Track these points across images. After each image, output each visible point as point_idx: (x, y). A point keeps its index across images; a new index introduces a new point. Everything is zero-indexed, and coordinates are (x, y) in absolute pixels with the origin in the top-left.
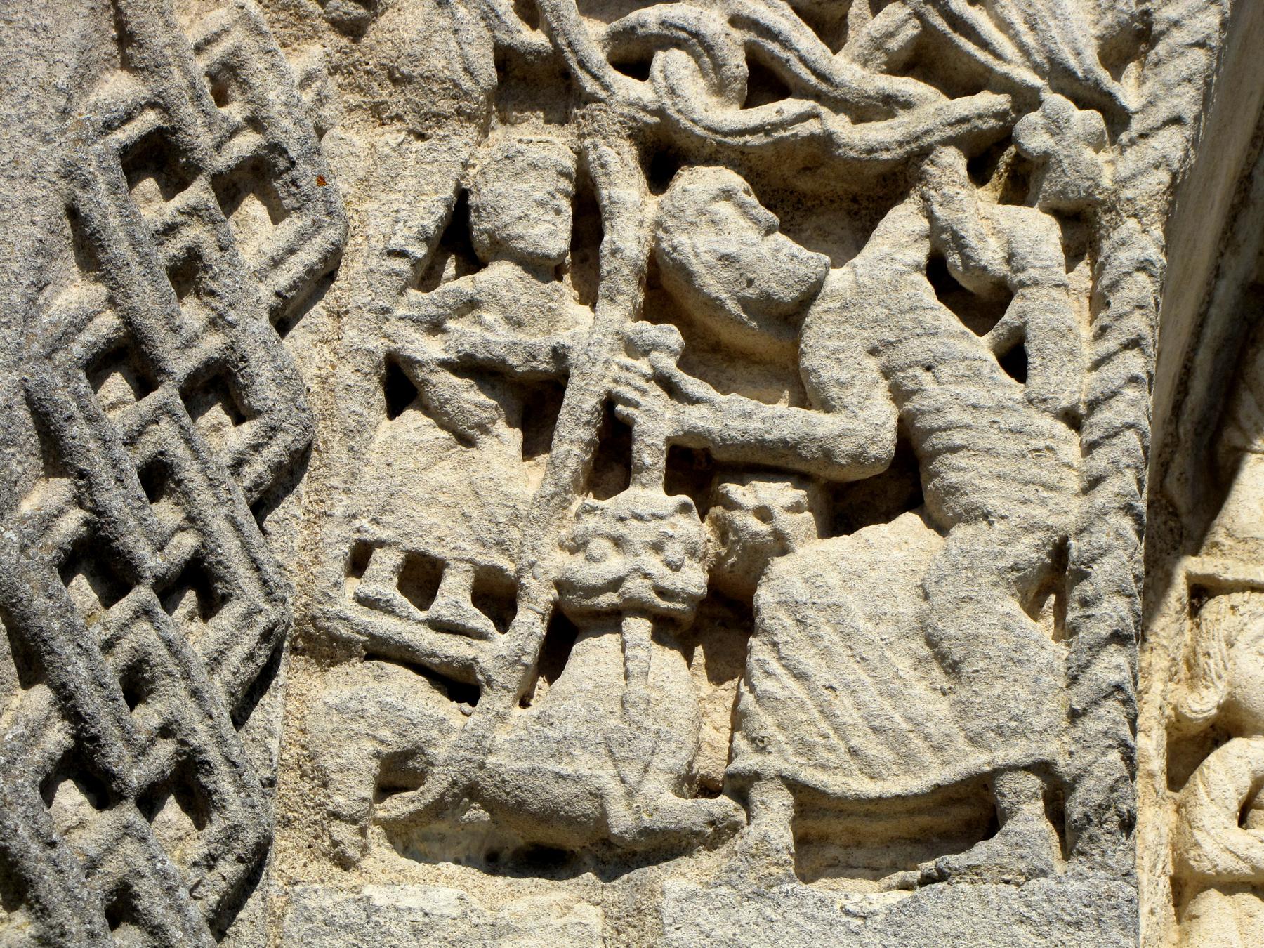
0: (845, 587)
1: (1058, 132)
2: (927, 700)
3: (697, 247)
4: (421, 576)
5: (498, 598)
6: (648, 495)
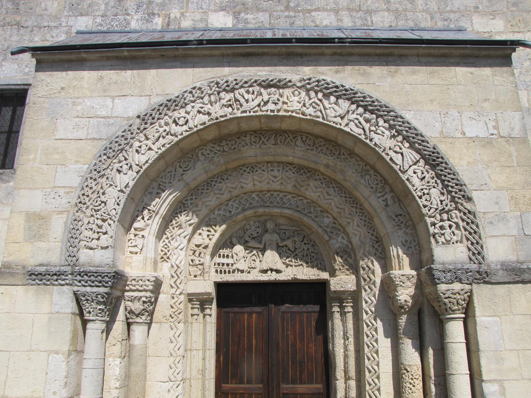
0: (103, 237)
1: (113, 218)
2: (106, 243)
3: (98, 223)
4: (87, 237)
5: (90, 238)
6: (96, 234)
